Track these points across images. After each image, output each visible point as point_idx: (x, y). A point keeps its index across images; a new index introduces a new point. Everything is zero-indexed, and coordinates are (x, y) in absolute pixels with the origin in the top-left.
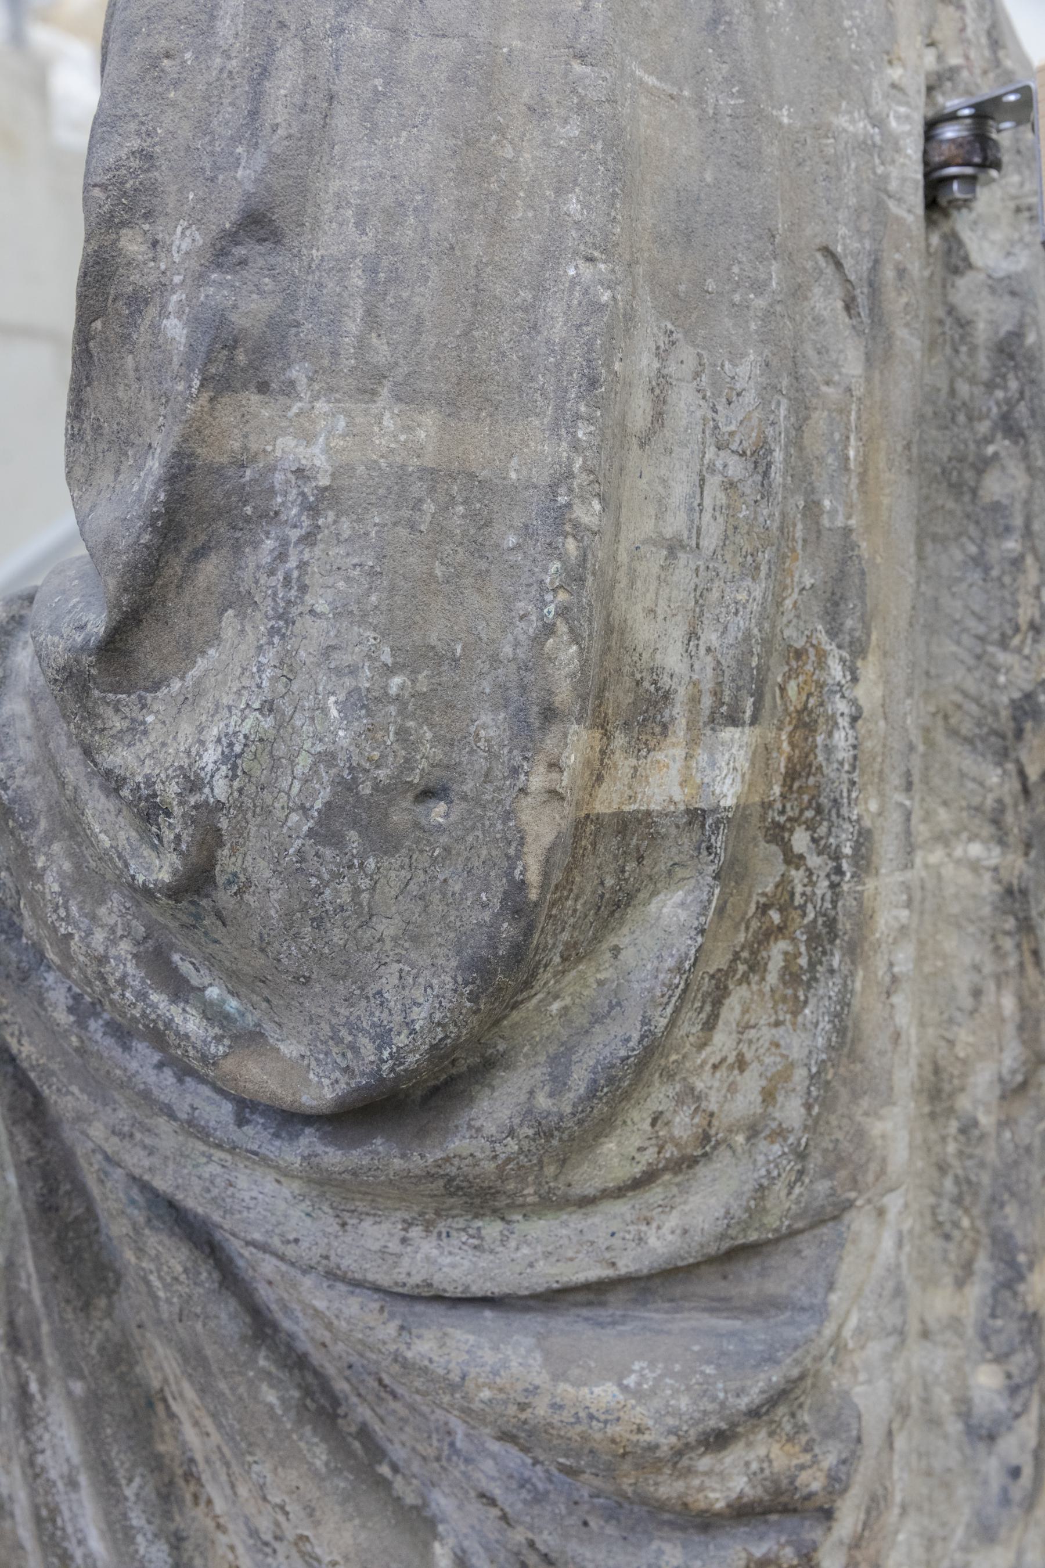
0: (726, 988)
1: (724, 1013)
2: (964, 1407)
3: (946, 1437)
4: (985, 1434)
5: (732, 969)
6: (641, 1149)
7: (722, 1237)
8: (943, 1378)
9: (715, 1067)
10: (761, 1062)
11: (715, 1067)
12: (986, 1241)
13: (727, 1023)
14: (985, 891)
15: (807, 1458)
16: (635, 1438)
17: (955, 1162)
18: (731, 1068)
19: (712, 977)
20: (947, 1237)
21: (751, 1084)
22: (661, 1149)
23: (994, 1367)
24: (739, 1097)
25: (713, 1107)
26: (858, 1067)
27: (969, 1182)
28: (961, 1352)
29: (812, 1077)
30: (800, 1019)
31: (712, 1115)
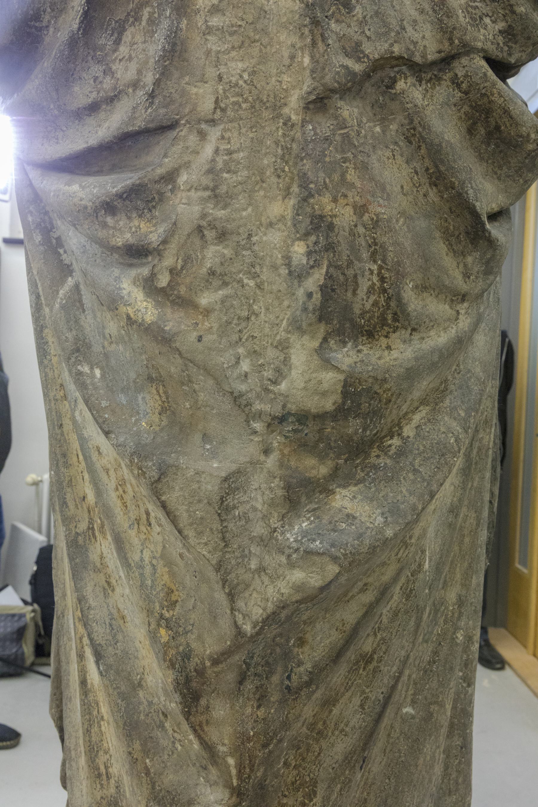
0: (124, 27)
1: (124, 38)
2: (288, 259)
3: (279, 275)
4: (298, 275)
5: (126, 20)
6: (91, 92)
7: (119, 129)
8: (278, 245)
9: (120, 60)
10: (138, 58)
11: (120, 60)
12: (296, 178)
13: (125, 42)
14: (297, 8)
15: (153, 229)
16: (80, 203)
17: (282, 139)
18: (127, 60)
19: (116, 22)
20: (279, 177)
21: (133, 67)
22: (99, 92)
23: (302, 243)
24: (129, 72)
25: (119, 76)
26: (186, 64)
27: (287, 148)
28: (286, 233)
29: (156, 62)
30: (153, 39)
31: (118, 79)
